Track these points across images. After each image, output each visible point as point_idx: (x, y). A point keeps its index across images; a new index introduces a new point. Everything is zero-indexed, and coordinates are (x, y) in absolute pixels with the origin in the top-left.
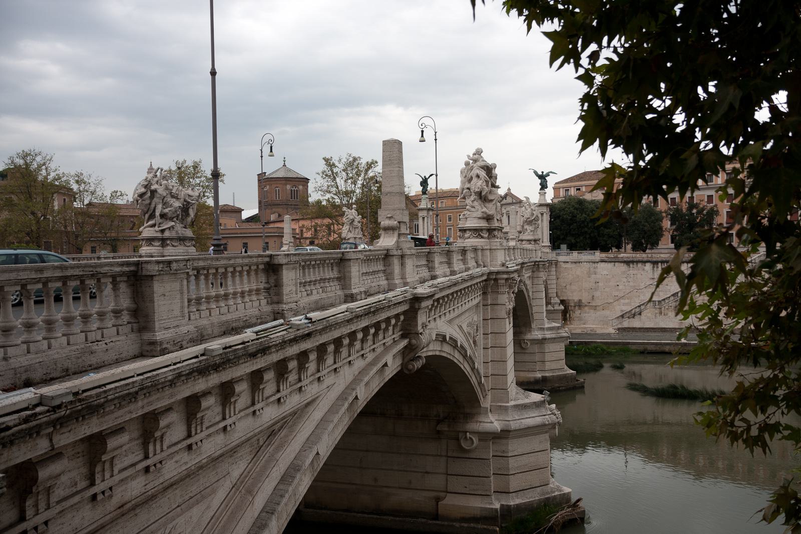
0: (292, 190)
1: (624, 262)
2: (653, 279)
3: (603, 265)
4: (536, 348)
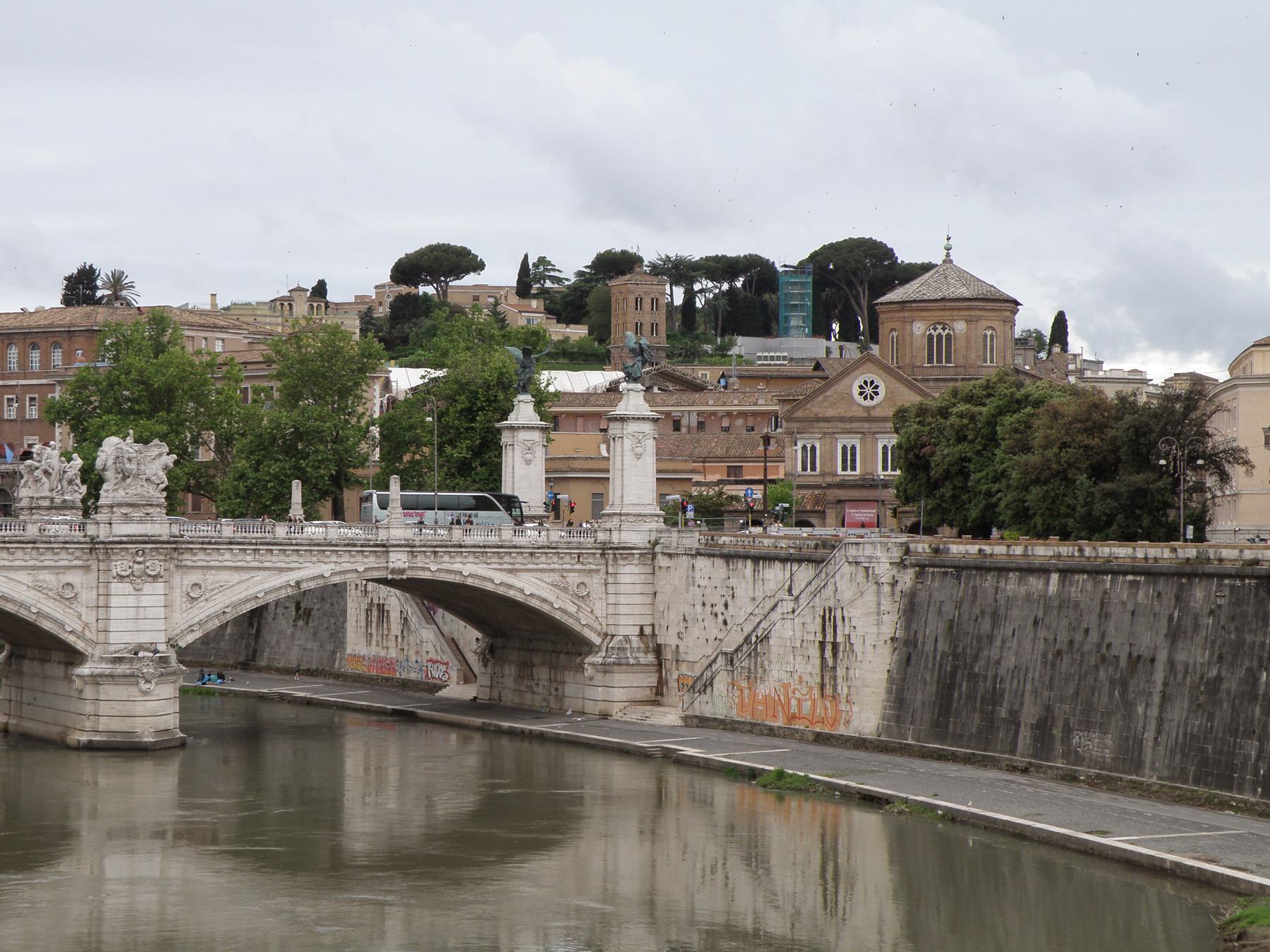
0: (930, 337)
1: (723, 556)
2: (754, 599)
3: (701, 562)
4: (89, 692)
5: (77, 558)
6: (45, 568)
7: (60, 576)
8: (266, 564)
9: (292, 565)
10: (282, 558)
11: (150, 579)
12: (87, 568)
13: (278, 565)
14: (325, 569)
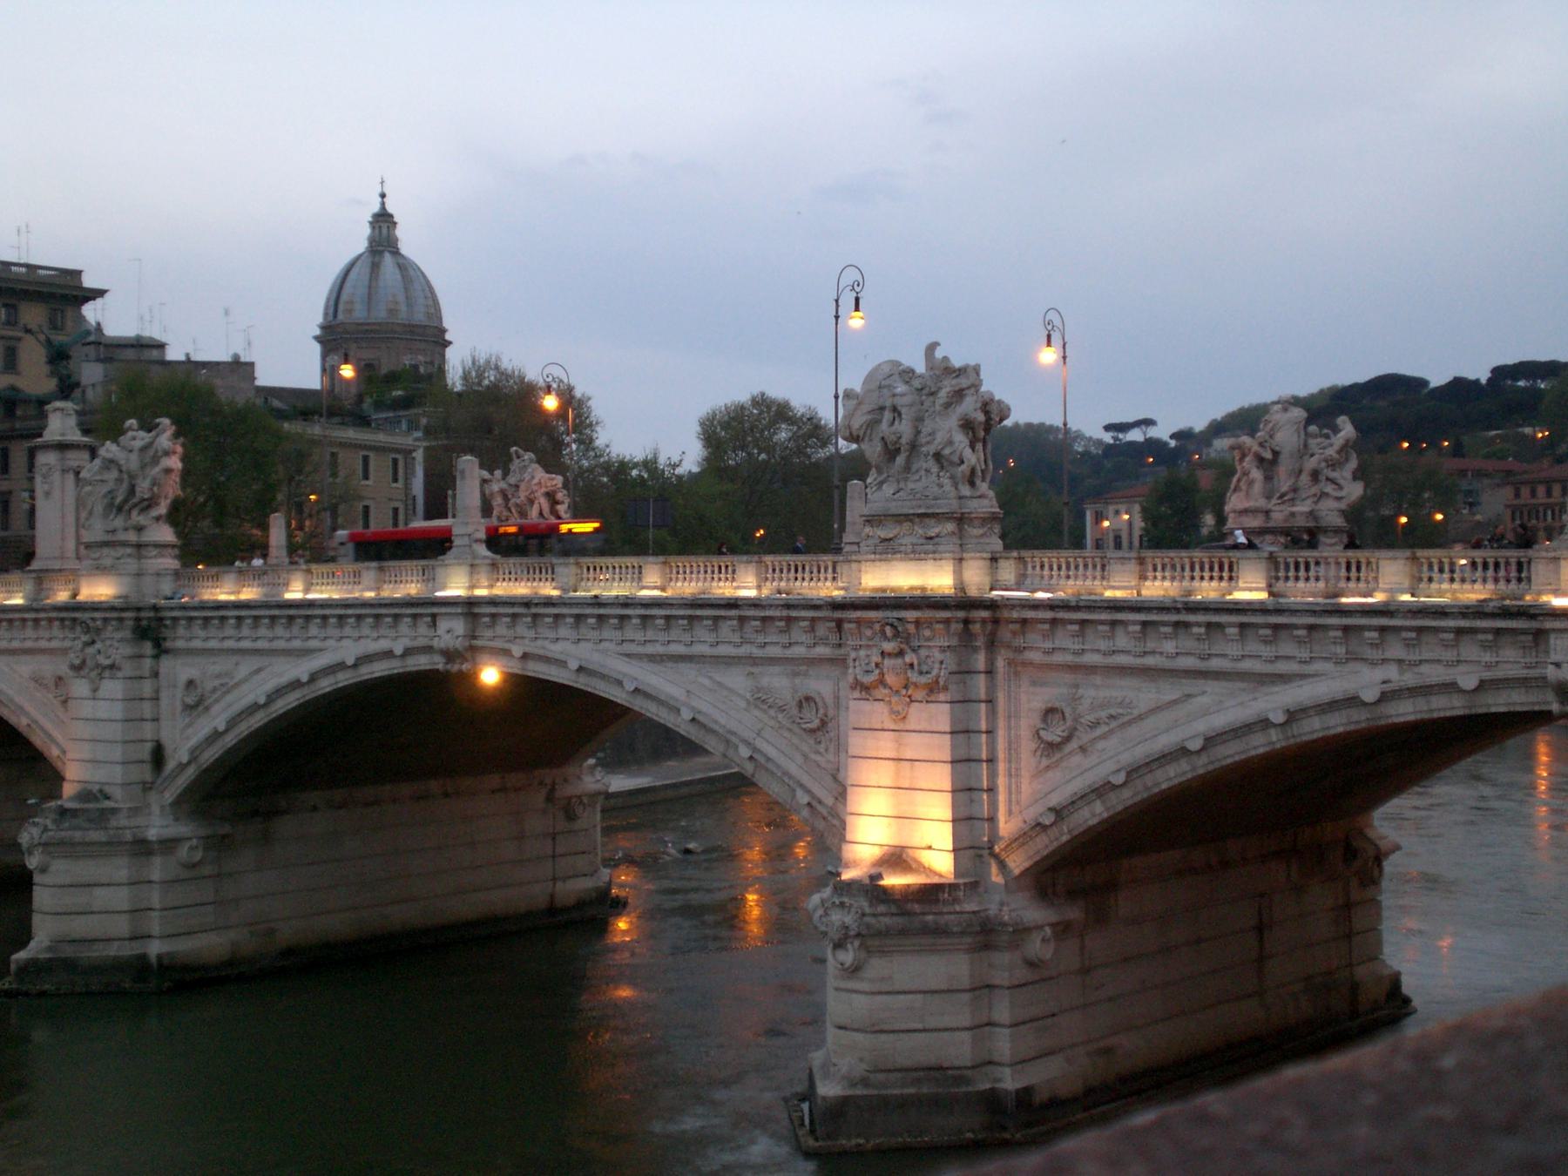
5: (824, 641)
6: (772, 661)
7: (797, 681)
8: (1215, 664)
9: (1282, 667)
10: (1253, 647)
11: (919, 695)
12: (841, 662)
13: (1246, 665)
14: (1366, 681)
